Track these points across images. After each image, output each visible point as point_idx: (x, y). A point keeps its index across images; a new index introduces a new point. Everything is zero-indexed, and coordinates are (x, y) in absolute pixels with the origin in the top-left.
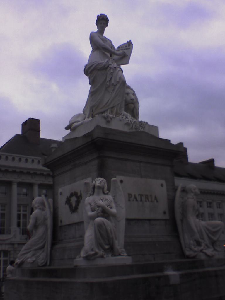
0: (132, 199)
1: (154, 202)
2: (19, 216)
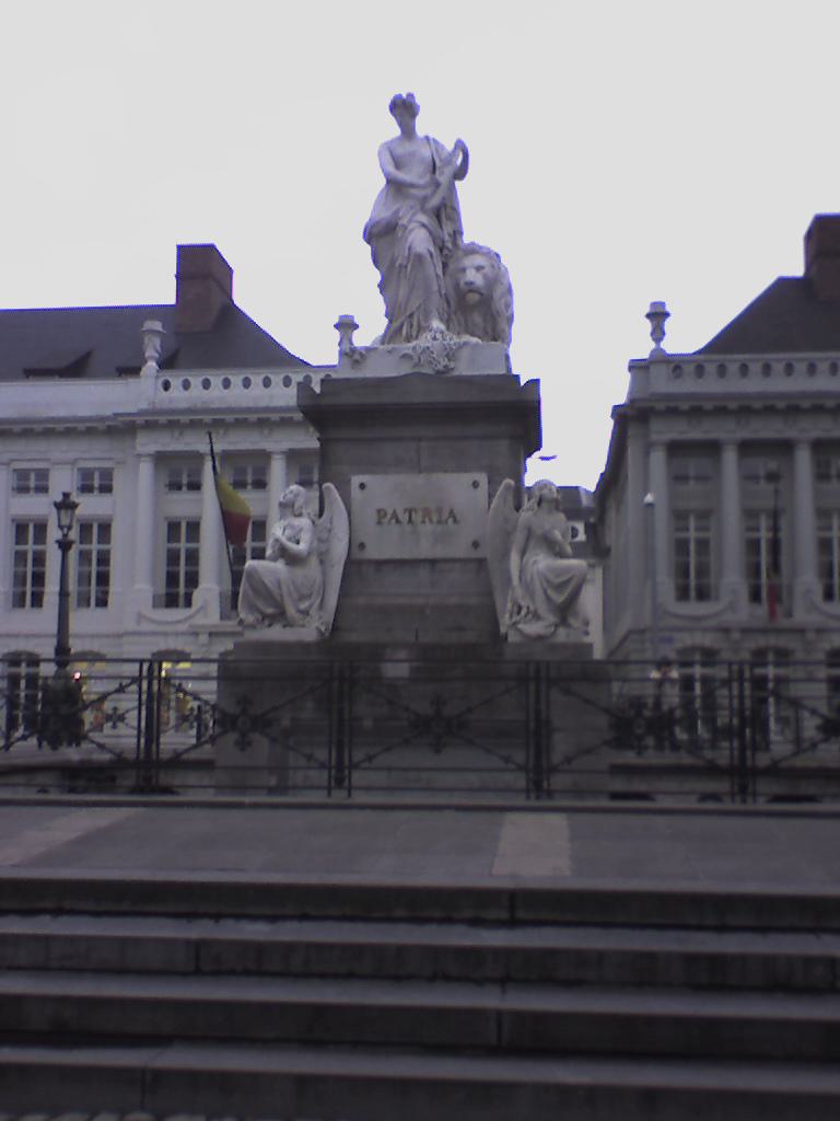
0: (386, 520)
1: (446, 522)
2: (681, 547)
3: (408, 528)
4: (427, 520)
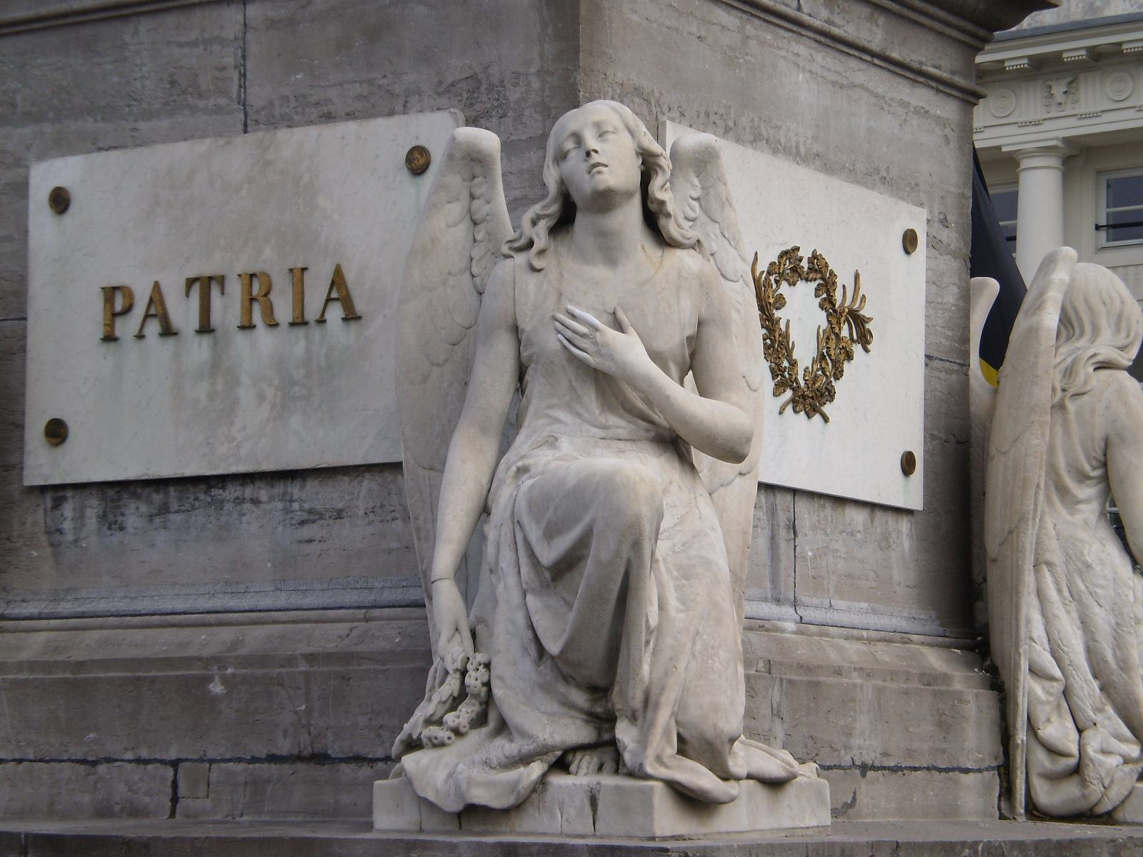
0: (127, 327)
1: (321, 321)
3: (199, 350)
4: (257, 318)
